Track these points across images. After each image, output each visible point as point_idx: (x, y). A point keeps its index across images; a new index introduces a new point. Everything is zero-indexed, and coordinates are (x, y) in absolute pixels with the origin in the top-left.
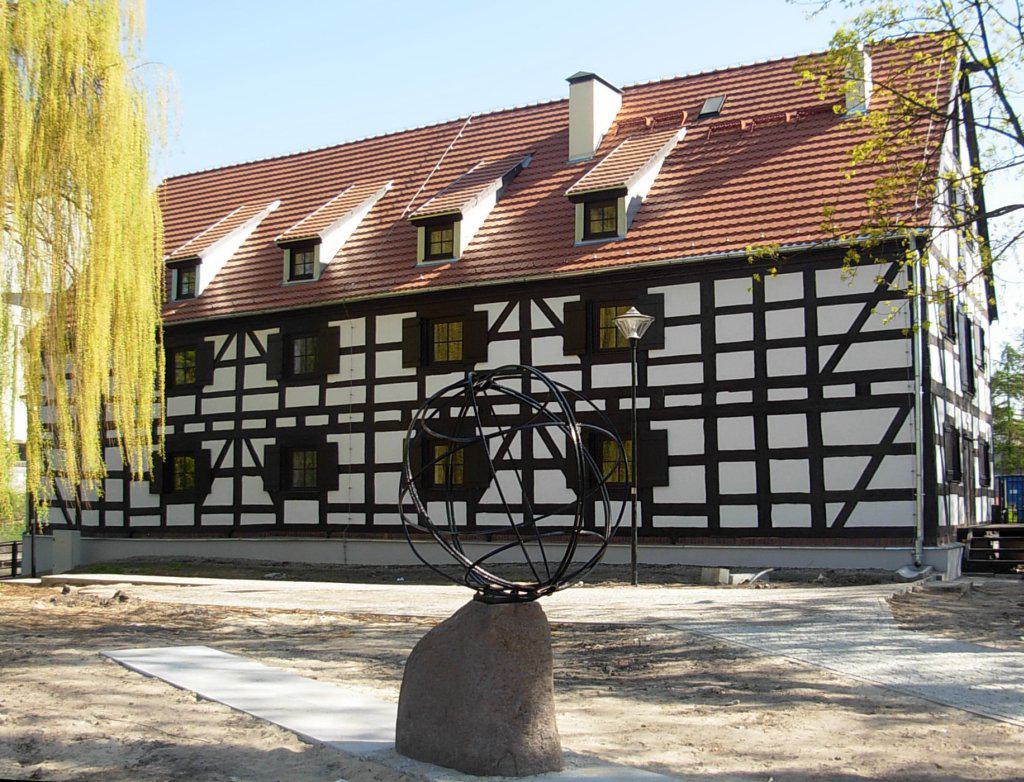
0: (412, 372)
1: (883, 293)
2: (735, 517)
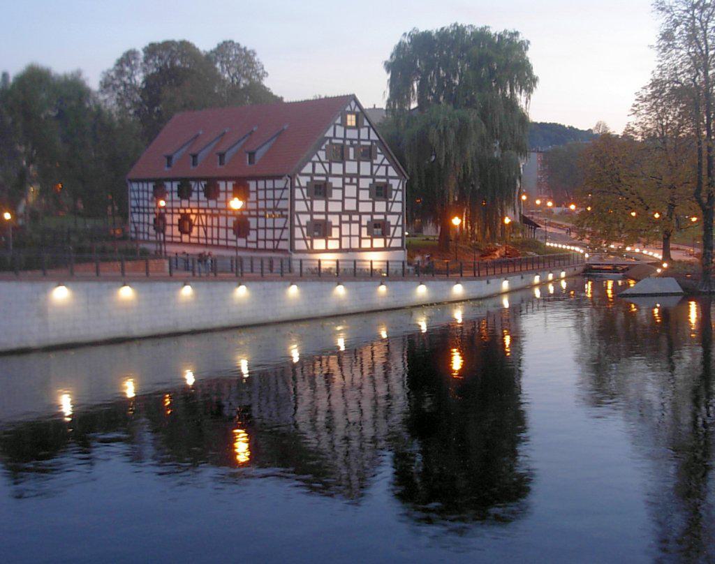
0: (206, 199)
1: (285, 188)
2: (261, 245)
